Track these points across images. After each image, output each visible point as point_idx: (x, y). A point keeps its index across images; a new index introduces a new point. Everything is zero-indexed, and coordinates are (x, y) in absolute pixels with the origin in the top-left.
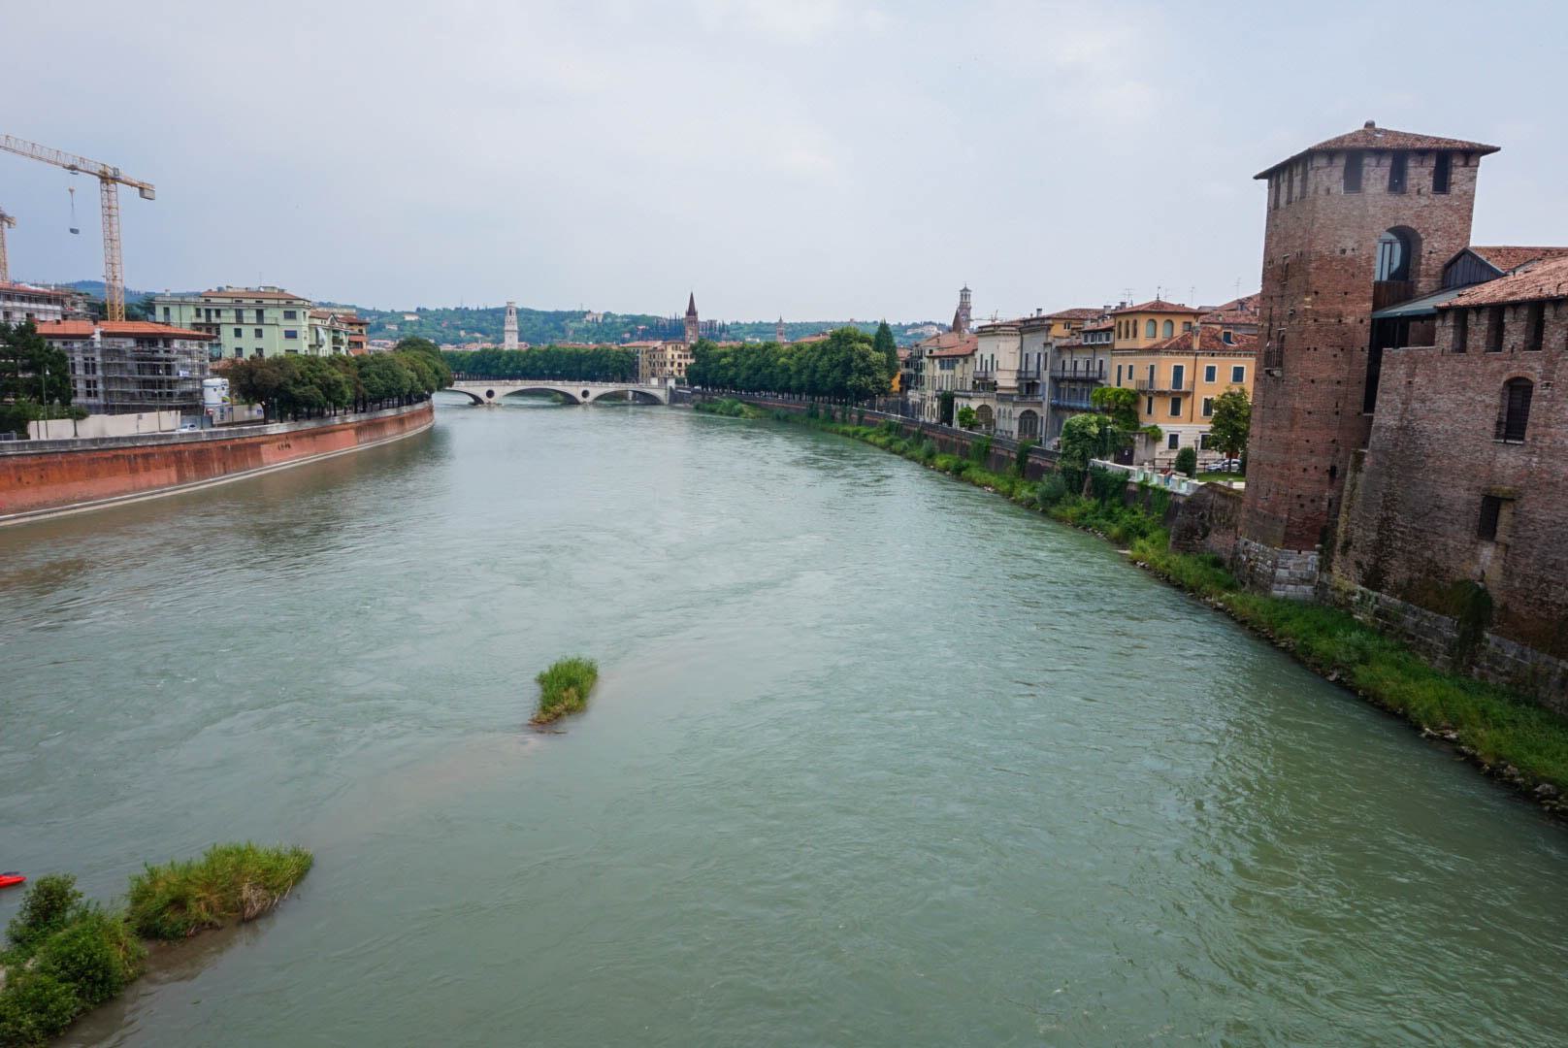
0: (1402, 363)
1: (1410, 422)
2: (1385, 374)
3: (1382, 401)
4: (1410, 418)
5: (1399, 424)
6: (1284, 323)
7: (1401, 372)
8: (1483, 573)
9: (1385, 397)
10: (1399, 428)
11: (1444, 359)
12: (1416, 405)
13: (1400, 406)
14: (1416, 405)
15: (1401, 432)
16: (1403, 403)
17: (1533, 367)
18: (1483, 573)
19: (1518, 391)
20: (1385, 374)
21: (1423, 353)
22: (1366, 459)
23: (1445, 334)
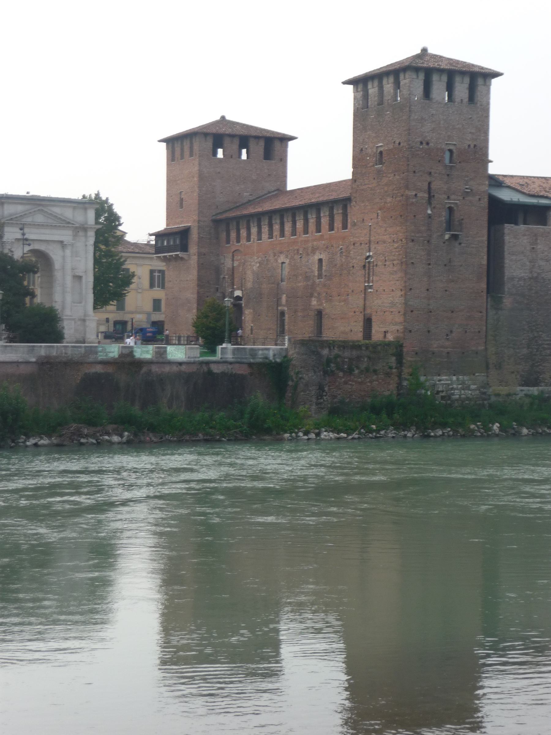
0: (524, 235)
1: (539, 274)
2: (509, 242)
4: (539, 271)
5: (530, 275)
6: (453, 197)
7: (525, 241)
9: (514, 257)
10: (530, 278)
12: (542, 263)
13: (528, 263)
14: (542, 263)
15: (532, 280)
16: (530, 262)
20: (509, 242)
21: (541, 230)
22: (505, 301)
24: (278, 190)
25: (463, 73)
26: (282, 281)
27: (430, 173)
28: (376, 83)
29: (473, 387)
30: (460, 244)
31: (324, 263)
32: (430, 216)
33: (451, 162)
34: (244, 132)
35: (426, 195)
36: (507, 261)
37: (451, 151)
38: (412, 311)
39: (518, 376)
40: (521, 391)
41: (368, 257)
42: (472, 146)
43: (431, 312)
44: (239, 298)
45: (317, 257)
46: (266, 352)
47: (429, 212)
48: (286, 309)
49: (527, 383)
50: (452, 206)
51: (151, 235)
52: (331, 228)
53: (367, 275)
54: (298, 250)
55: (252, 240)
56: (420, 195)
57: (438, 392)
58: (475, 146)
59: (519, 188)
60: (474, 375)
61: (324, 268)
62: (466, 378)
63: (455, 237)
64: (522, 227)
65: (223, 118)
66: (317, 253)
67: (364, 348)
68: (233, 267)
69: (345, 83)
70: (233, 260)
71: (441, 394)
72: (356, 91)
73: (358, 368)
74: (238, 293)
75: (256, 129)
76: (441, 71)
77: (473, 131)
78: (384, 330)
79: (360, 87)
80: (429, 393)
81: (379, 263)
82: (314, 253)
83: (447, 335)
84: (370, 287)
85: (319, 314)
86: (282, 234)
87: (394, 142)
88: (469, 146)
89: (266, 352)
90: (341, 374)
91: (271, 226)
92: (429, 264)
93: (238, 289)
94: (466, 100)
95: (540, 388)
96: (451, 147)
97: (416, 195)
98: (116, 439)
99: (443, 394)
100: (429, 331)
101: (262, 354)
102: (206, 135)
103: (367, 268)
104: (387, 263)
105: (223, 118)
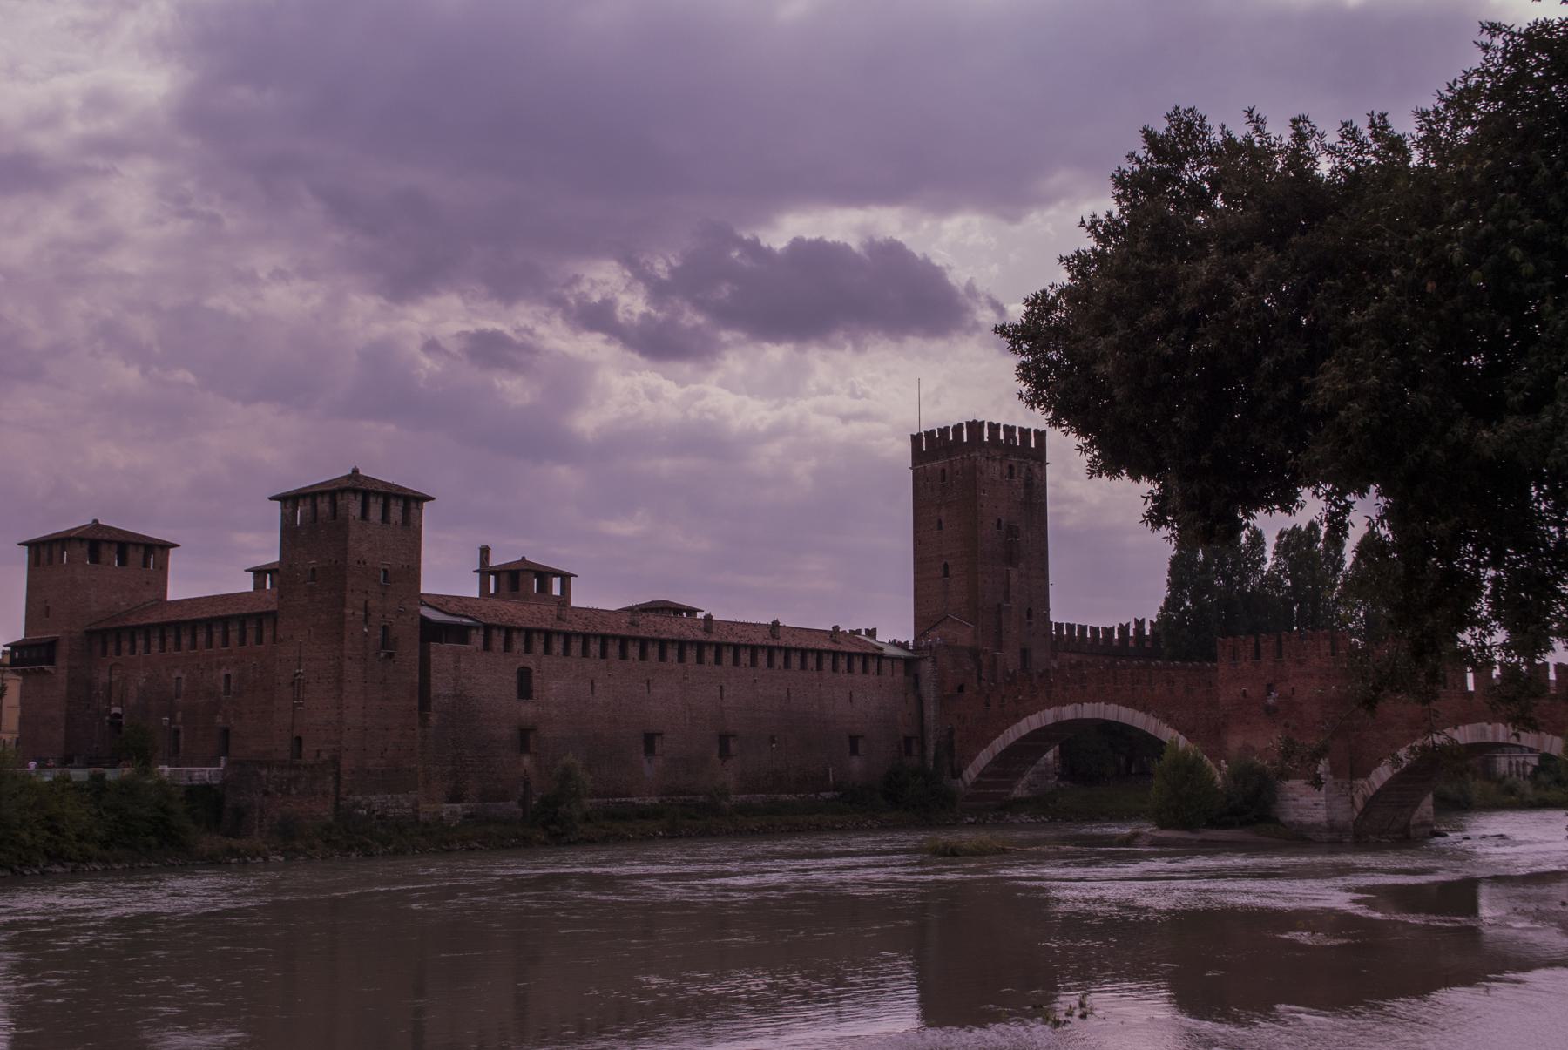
0: (448, 653)
3: (437, 678)
5: (453, 693)
6: (387, 615)
8: (525, 771)
9: (439, 675)
11: (479, 653)
12: (464, 681)
14: (464, 681)
17: (530, 661)
18: (525, 771)
19: (524, 675)
23: (477, 638)
24: (157, 600)
25: (397, 496)
26: (177, 697)
27: (366, 592)
28: (309, 501)
29: (407, 805)
30: (394, 662)
31: (232, 680)
32: (366, 634)
33: (385, 580)
34: (121, 538)
35: (363, 614)
36: (432, 679)
37: (385, 571)
38: (349, 729)
39: (444, 793)
40: (446, 809)
41: (297, 675)
42: (405, 566)
43: (366, 730)
44: (117, 716)
45: (223, 672)
46: (202, 773)
47: (366, 630)
48: (182, 727)
49: (452, 800)
50: (387, 624)
51: (5, 646)
52: (242, 641)
53: (296, 693)
54: (198, 665)
55: (137, 652)
56: (356, 613)
57: (374, 811)
58: (408, 566)
59: (439, 607)
60: (407, 792)
61: (232, 684)
62: (400, 796)
63: (390, 655)
64: (447, 645)
65: (95, 521)
66: (224, 668)
67: (302, 768)
68: (111, 682)
69: (271, 499)
70: (110, 675)
71: (376, 813)
72: (284, 507)
73: (296, 788)
74: (116, 710)
75: (160, 541)
76: (377, 494)
77: (407, 552)
78: (317, 748)
79: (289, 504)
80: (365, 812)
81: (311, 680)
82: (220, 669)
83: (382, 753)
84: (301, 705)
85: (226, 733)
86: (178, 646)
87: (330, 561)
88: (403, 566)
89: (202, 773)
90: (280, 795)
91: (163, 639)
92: (366, 682)
93: (117, 705)
94: (400, 522)
95: (464, 804)
96: (386, 567)
97: (353, 613)
98: (59, 869)
99: (379, 813)
100: (364, 750)
101: (200, 776)
102: (81, 540)
103: (296, 686)
104: (321, 681)
105: (95, 521)
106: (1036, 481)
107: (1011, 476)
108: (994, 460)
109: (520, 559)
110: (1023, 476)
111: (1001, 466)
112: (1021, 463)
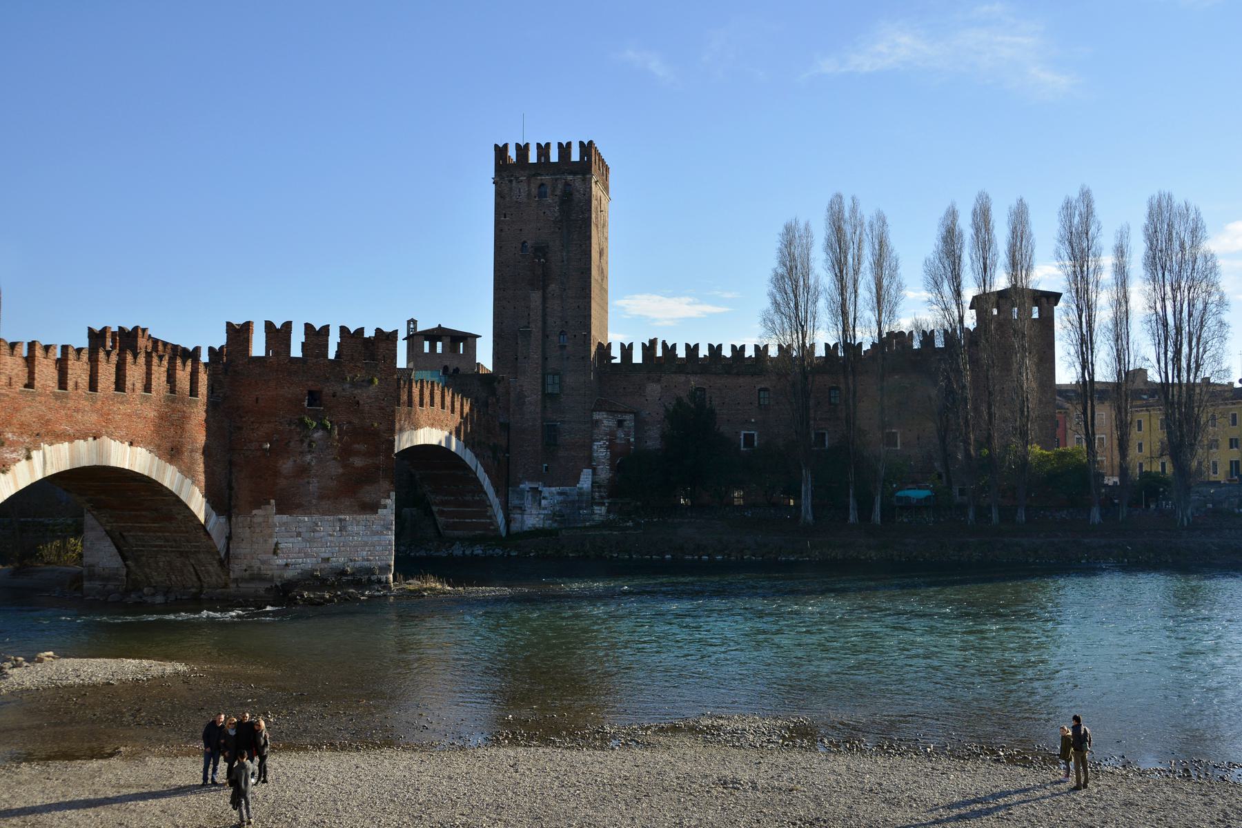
106: (577, 196)
107: (542, 195)
108: (519, 182)
109: (437, 326)
110: (558, 192)
111: (529, 186)
112: (556, 180)
